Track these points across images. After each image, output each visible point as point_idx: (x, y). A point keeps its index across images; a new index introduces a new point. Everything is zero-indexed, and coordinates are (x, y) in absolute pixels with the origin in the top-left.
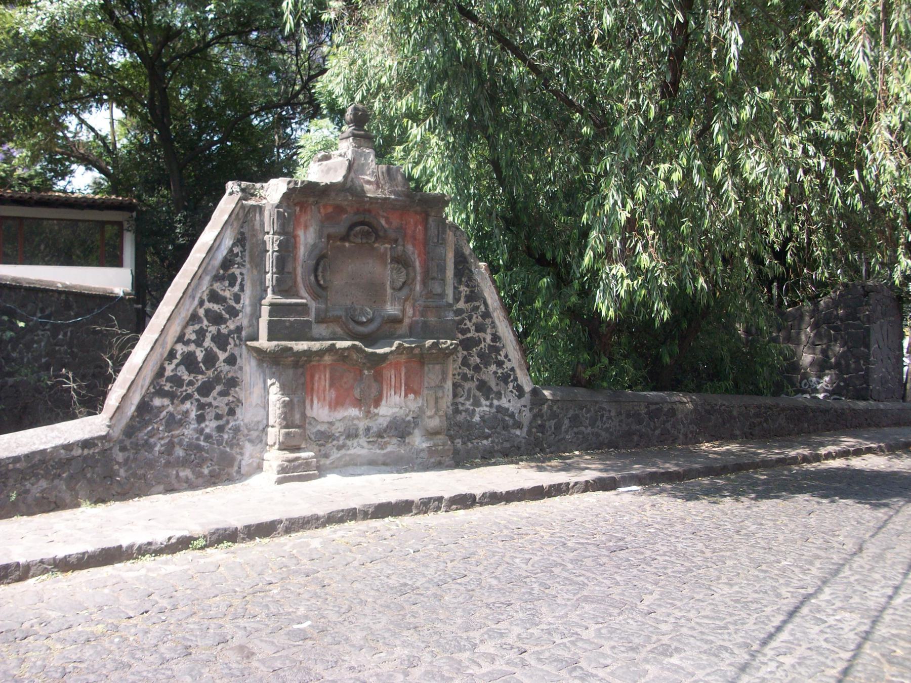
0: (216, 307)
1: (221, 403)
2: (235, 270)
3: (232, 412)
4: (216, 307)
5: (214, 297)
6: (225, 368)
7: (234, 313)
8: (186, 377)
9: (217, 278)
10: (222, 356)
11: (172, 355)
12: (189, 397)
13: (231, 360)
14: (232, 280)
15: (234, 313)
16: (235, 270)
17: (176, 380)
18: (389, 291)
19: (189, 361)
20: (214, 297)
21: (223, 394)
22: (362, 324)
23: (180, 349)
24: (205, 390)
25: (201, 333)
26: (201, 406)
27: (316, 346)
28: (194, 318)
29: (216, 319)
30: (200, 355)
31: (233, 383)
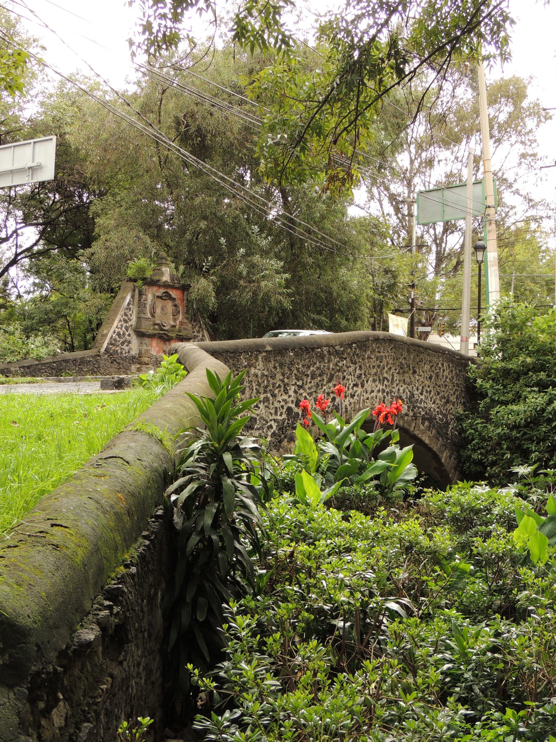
0: (126, 318)
1: (127, 348)
2: (131, 306)
3: (129, 352)
4: (126, 318)
5: (126, 314)
6: (128, 337)
7: (130, 320)
8: (118, 339)
9: (127, 309)
10: (127, 333)
11: (114, 332)
12: (118, 346)
13: (129, 335)
14: (130, 309)
15: (130, 320)
16: (131, 306)
17: (115, 340)
18: (172, 317)
19: (119, 334)
20: (126, 314)
21: (127, 346)
22: (164, 326)
23: (117, 330)
24: (123, 344)
25: (122, 325)
26: (122, 349)
27: (155, 332)
28: (120, 321)
29: (126, 321)
30: (121, 333)
31: (129, 342)
